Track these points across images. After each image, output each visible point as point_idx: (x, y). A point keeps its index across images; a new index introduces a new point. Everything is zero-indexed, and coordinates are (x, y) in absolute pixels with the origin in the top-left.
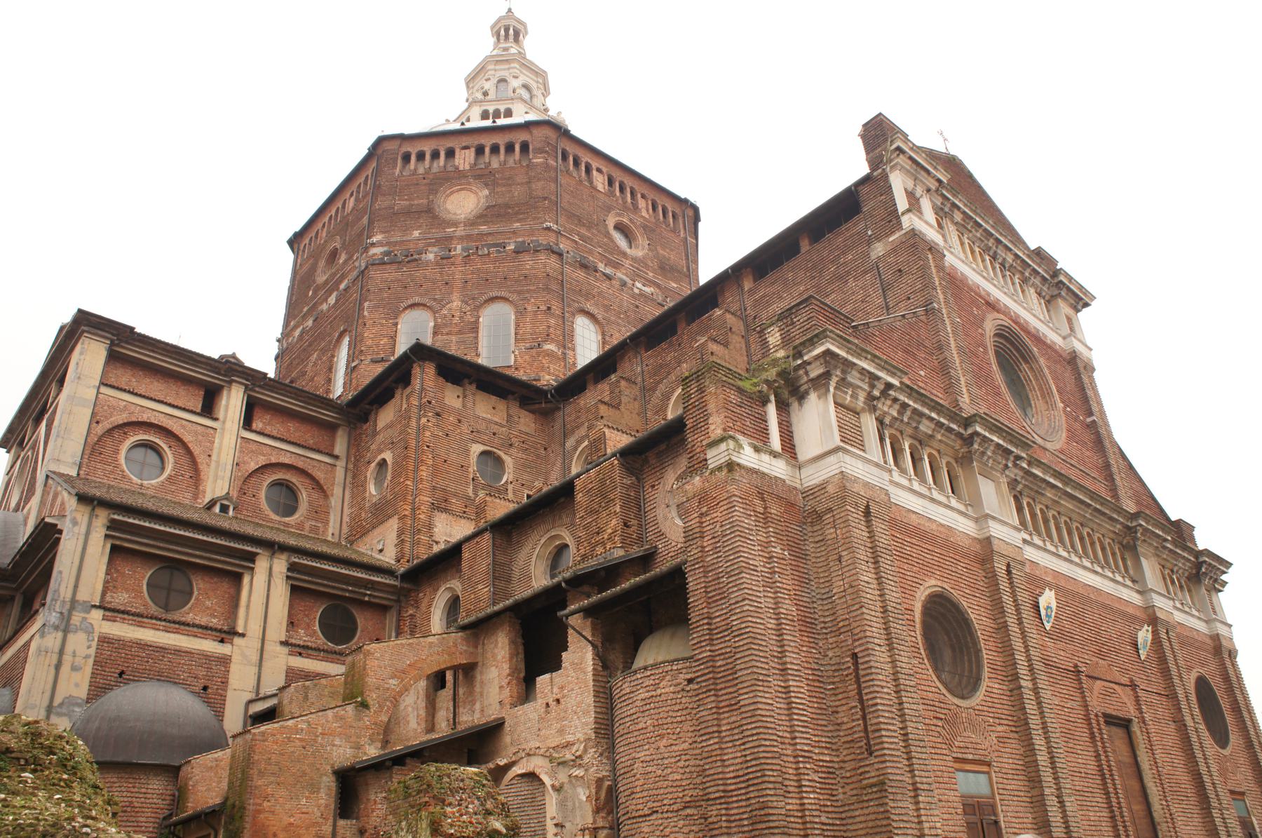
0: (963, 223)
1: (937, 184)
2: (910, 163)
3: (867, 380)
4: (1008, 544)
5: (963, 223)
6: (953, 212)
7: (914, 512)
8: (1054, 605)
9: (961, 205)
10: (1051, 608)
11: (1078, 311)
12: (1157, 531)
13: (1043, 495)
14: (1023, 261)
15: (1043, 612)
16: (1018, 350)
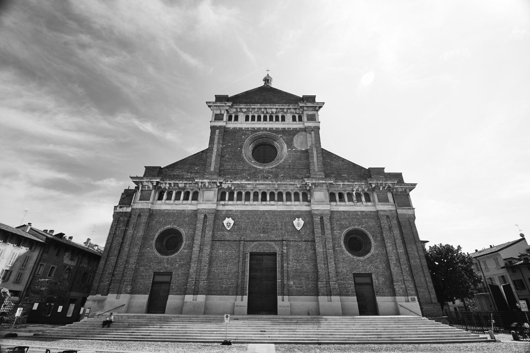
0: (247, 111)
1: (229, 107)
2: (215, 107)
3: (150, 183)
4: (206, 209)
5: (247, 111)
6: (242, 110)
7: (166, 210)
8: (232, 222)
9: (244, 107)
10: (230, 224)
11: (317, 111)
12: (321, 182)
13: (246, 187)
14: (280, 108)
15: (225, 225)
16: (271, 139)
